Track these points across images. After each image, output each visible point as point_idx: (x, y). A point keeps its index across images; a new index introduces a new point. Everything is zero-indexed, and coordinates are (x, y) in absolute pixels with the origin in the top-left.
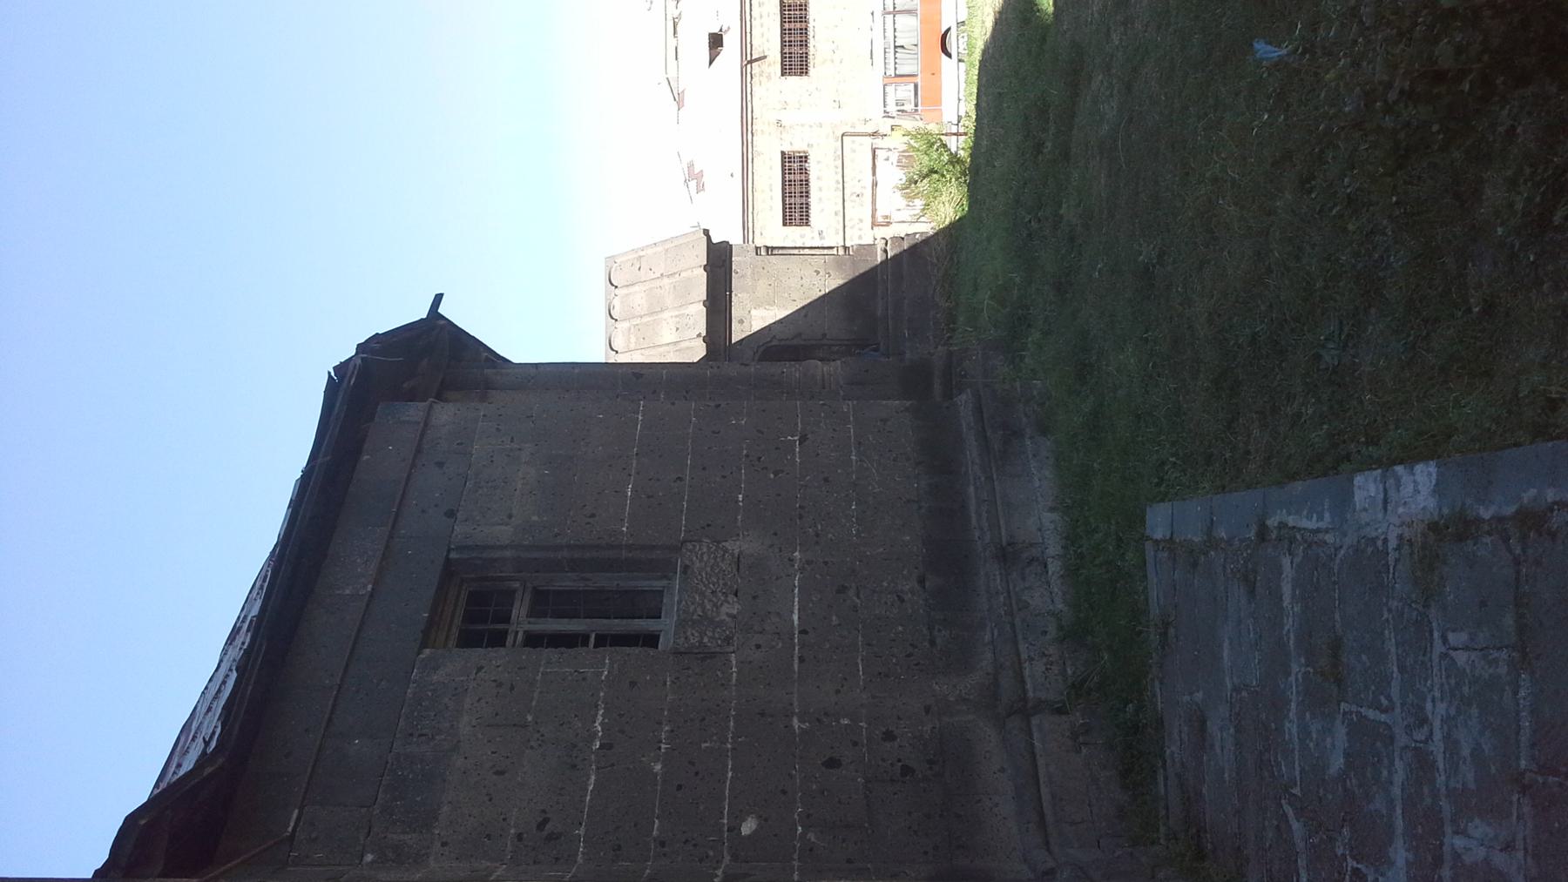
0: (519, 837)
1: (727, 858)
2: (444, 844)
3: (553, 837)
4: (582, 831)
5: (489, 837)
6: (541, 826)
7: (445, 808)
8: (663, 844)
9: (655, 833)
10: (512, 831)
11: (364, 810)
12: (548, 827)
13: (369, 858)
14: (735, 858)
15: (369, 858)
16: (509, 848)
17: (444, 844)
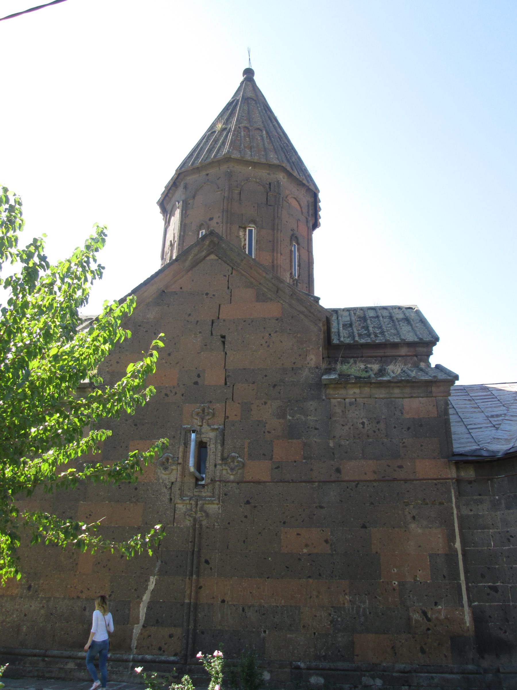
0: (508, 532)
1: (510, 585)
2: (503, 514)
3: (509, 540)
4: (511, 547)
5: (507, 524)
6: (511, 536)
7: (512, 511)
8: (511, 568)
9: (514, 566)
10: (509, 530)
11: (508, 491)
12: (511, 538)
13: (497, 497)
14: (511, 587)
15: (497, 497)
16: (504, 530)
17: (503, 514)
